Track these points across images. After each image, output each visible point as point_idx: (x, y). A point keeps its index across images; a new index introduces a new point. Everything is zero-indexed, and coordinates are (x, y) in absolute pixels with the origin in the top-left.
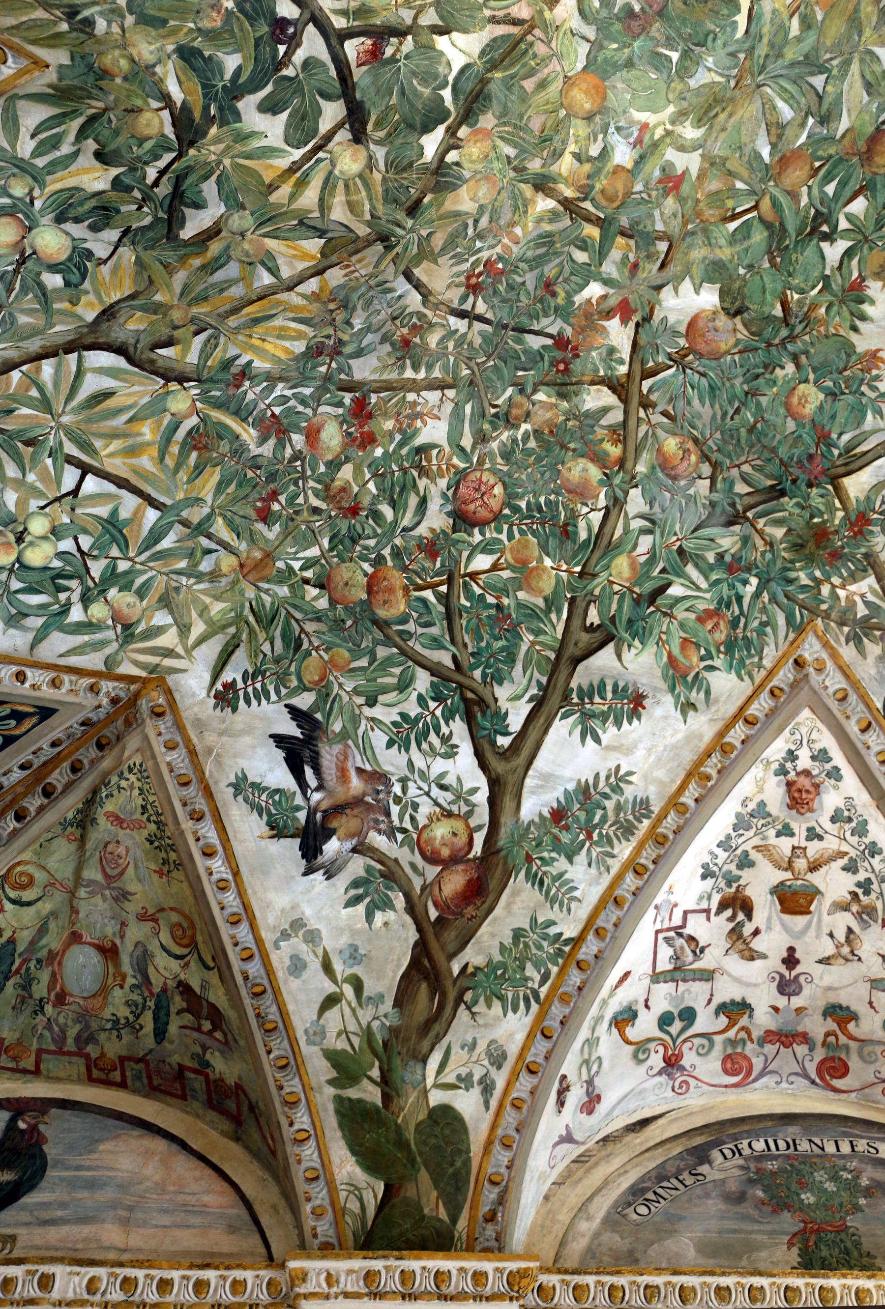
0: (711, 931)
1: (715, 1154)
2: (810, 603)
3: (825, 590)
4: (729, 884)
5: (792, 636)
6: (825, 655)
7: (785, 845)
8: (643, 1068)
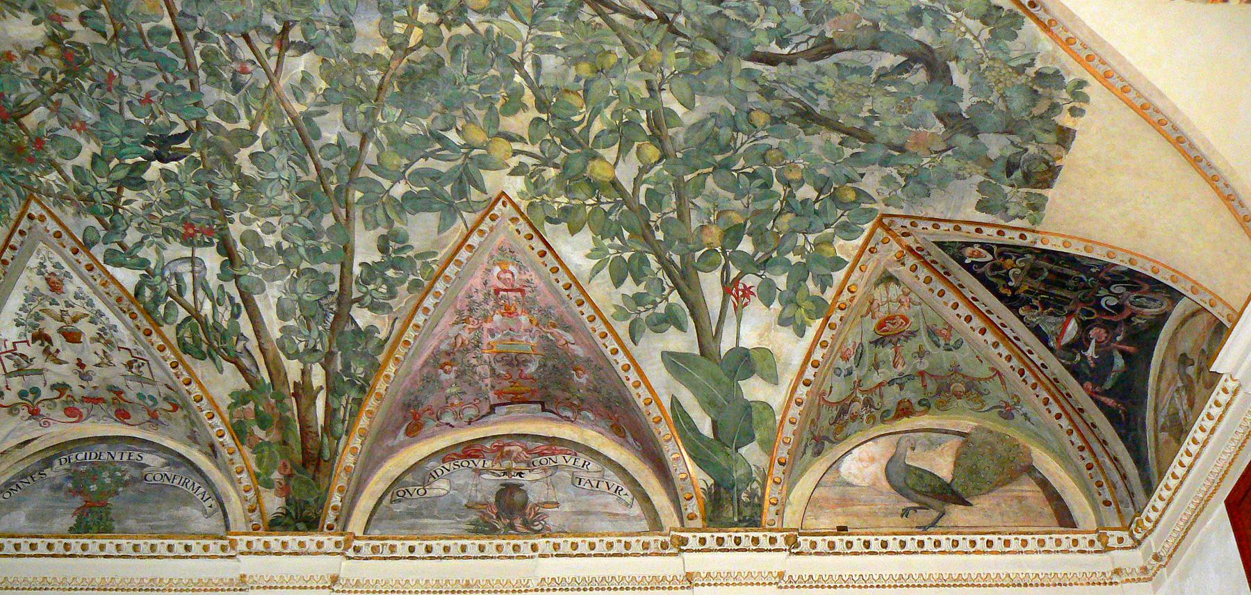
0: (33, 350)
1: (57, 462)
2: (26, 184)
3: (33, 178)
4: (34, 328)
5: (23, 202)
6: (44, 213)
7: (56, 309)
8: (18, 418)
